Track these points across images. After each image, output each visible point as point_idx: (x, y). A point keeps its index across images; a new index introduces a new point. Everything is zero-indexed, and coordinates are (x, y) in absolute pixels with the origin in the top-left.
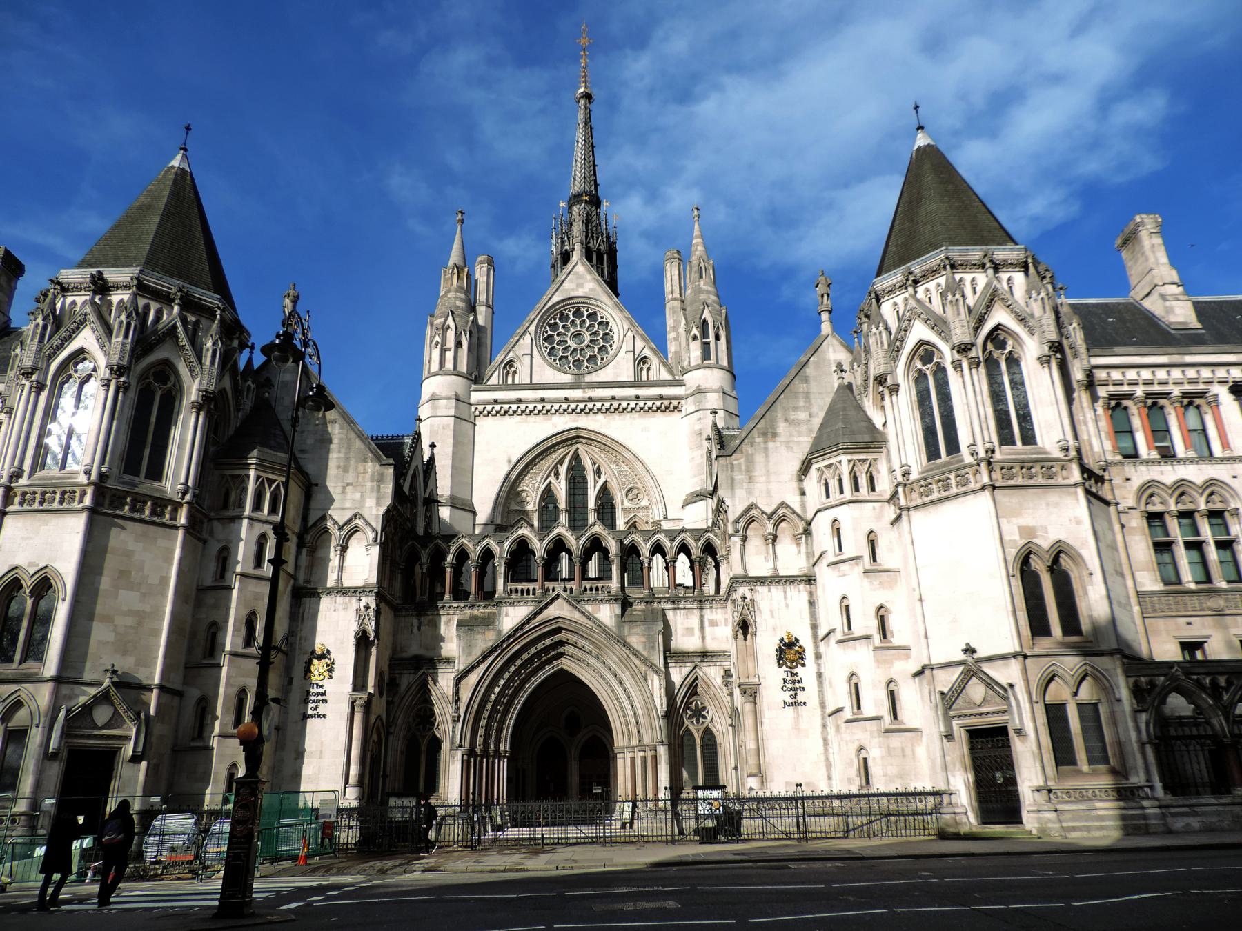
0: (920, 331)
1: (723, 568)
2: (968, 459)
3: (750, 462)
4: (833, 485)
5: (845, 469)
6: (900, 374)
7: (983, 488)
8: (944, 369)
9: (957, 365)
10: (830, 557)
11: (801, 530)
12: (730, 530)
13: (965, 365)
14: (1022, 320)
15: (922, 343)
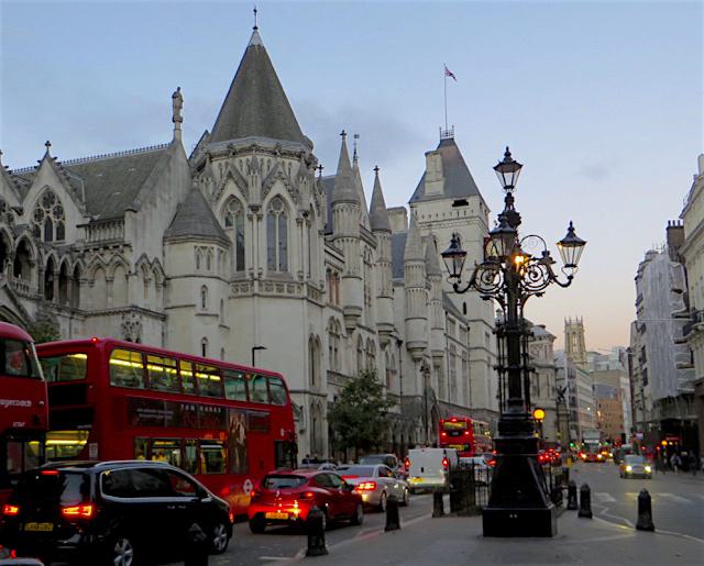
0: (278, 188)
1: (84, 290)
2: (296, 279)
3: (144, 217)
4: (203, 262)
5: (215, 252)
6: (264, 211)
7: (303, 299)
8: (286, 218)
9: (299, 222)
10: (199, 309)
11: (162, 281)
12: (133, 271)
13: (304, 223)
14: (318, 206)
15: (278, 196)
